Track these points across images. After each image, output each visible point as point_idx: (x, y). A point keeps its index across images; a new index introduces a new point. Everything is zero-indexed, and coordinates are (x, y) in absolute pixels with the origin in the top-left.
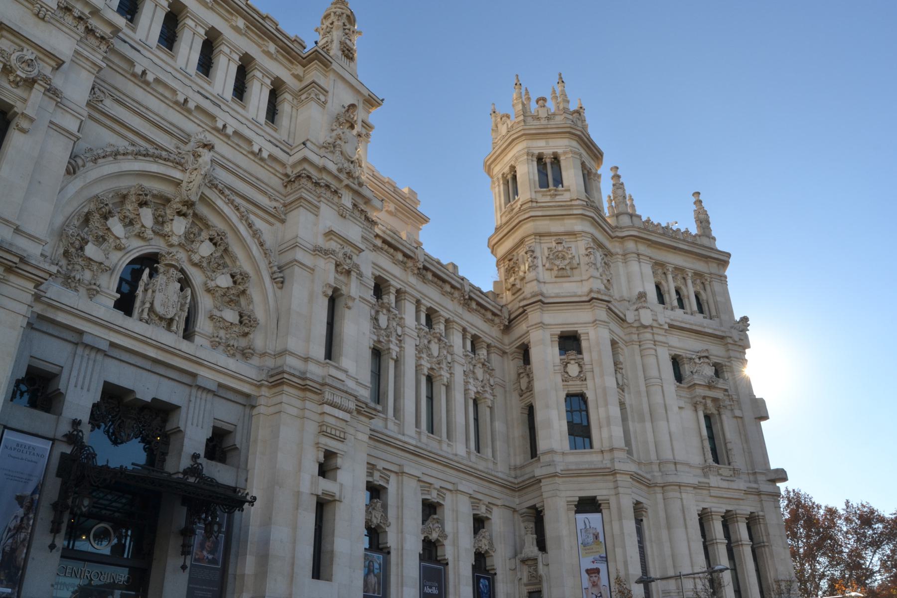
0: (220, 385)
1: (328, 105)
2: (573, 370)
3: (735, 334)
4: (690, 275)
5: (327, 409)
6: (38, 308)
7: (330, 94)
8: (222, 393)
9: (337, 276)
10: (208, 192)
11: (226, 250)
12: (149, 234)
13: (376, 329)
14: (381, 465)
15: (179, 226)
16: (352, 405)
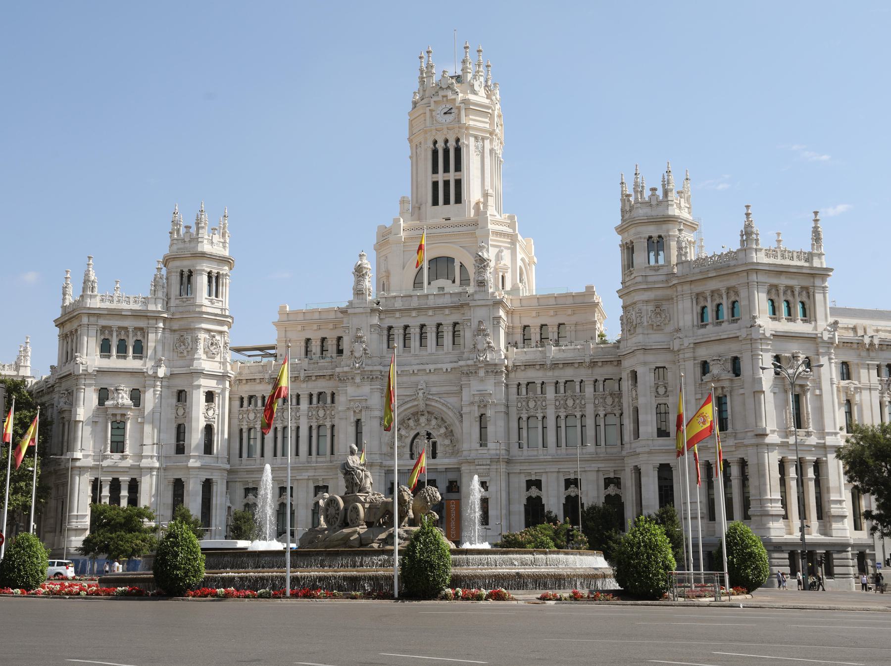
0: (446, 468)
1: (472, 326)
2: (634, 392)
3: (743, 334)
4: (723, 292)
5: (478, 467)
6: (386, 469)
7: (472, 320)
8: (448, 470)
9: (482, 410)
10: (428, 402)
11: (442, 419)
12: (414, 427)
13: (528, 411)
14: (533, 472)
15: (423, 420)
16: (488, 462)
